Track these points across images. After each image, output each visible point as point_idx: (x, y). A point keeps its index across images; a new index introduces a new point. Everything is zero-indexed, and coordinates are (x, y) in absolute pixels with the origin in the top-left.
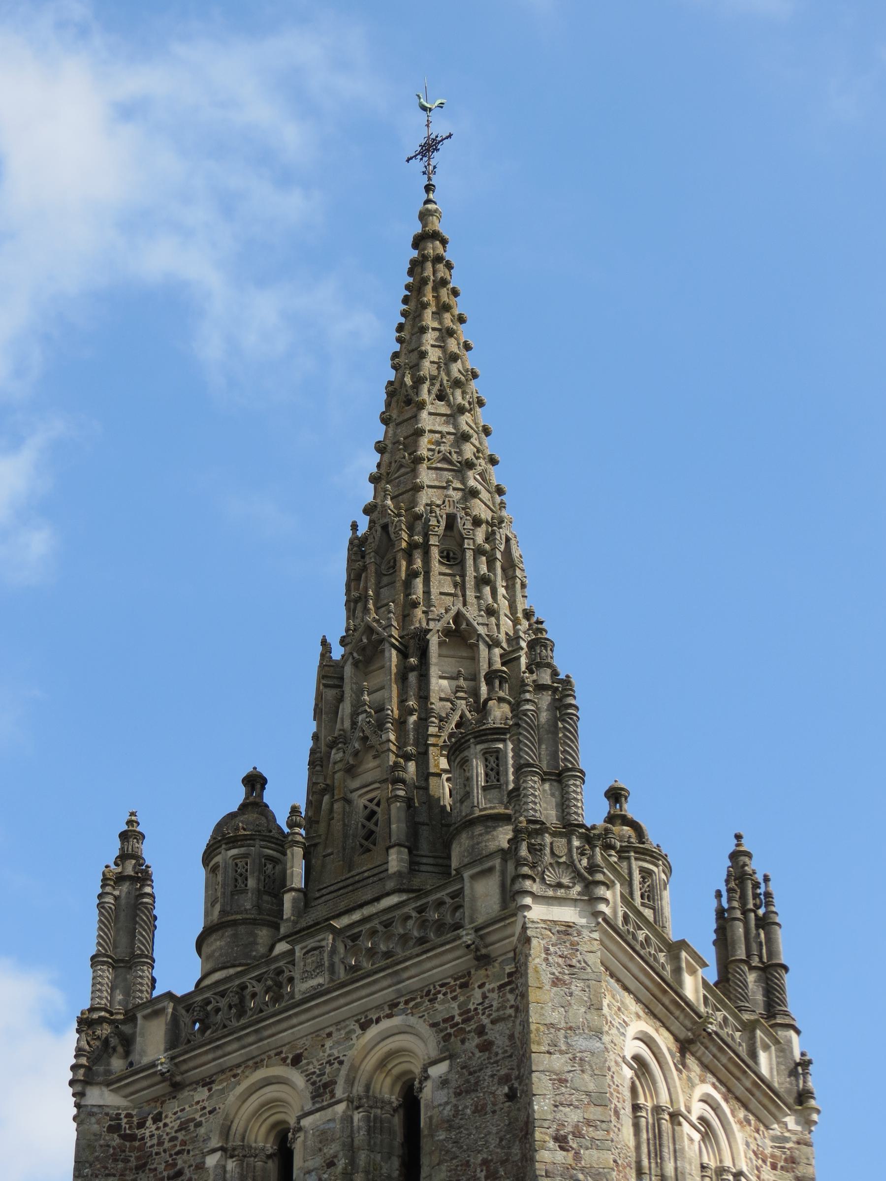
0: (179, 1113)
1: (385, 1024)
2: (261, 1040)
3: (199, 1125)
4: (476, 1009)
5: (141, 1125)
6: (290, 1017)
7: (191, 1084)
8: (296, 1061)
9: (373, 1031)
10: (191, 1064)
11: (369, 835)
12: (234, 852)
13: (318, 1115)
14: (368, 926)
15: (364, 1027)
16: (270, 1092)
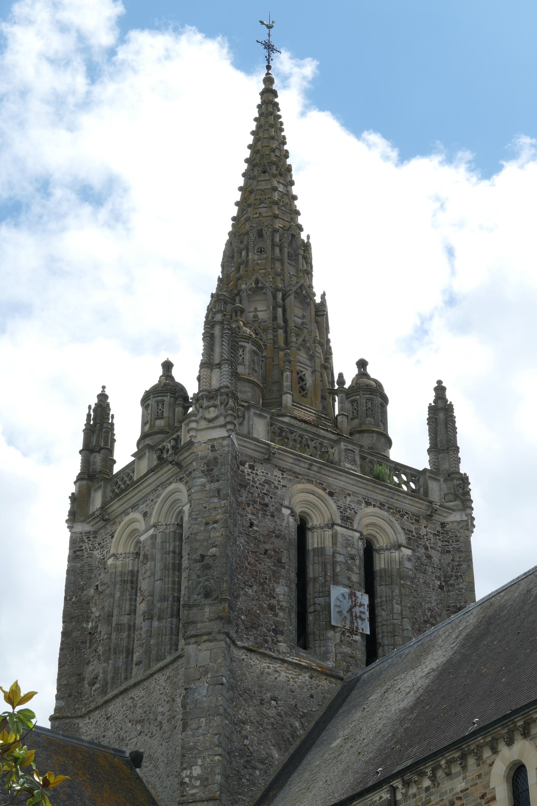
0: (265, 474)
1: (377, 510)
2: (318, 472)
3: (276, 488)
4: (423, 536)
5: (243, 465)
6: (333, 472)
7: (272, 464)
8: (331, 494)
9: (370, 509)
10: (325, 472)
11: (303, 389)
12: (255, 348)
13: (344, 529)
14: (371, 458)
15: (368, 504)
16: (311, 498)
